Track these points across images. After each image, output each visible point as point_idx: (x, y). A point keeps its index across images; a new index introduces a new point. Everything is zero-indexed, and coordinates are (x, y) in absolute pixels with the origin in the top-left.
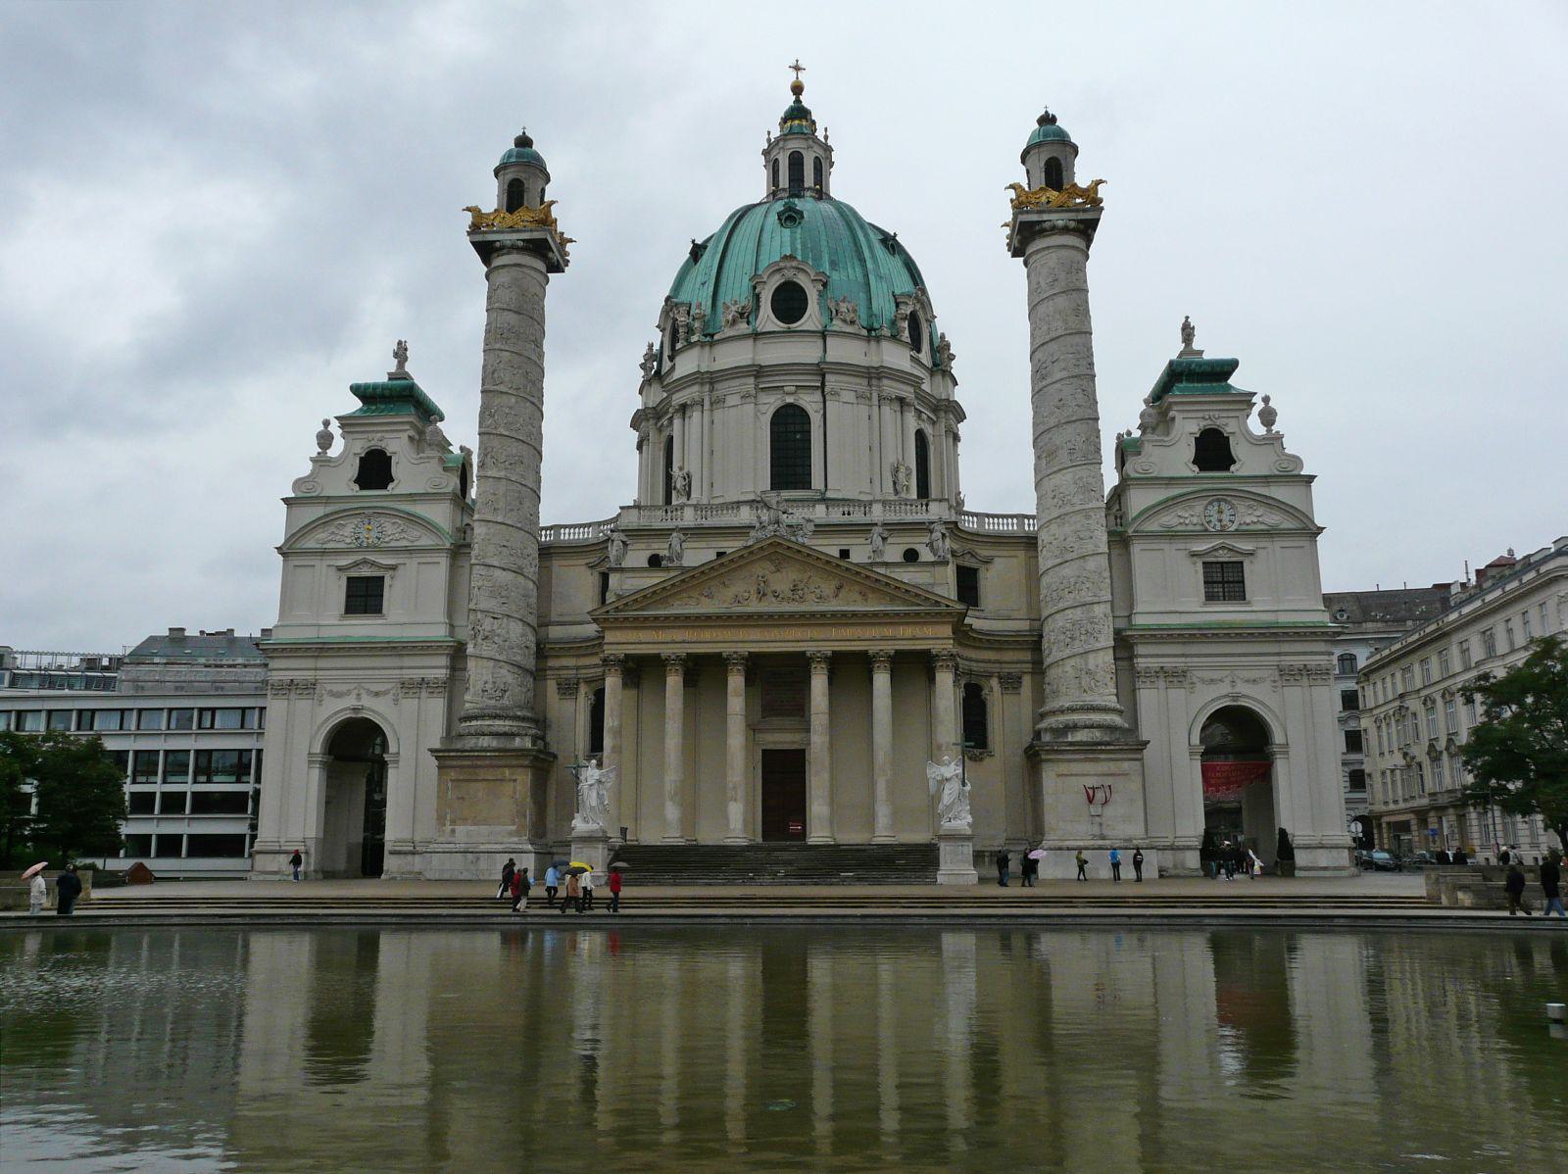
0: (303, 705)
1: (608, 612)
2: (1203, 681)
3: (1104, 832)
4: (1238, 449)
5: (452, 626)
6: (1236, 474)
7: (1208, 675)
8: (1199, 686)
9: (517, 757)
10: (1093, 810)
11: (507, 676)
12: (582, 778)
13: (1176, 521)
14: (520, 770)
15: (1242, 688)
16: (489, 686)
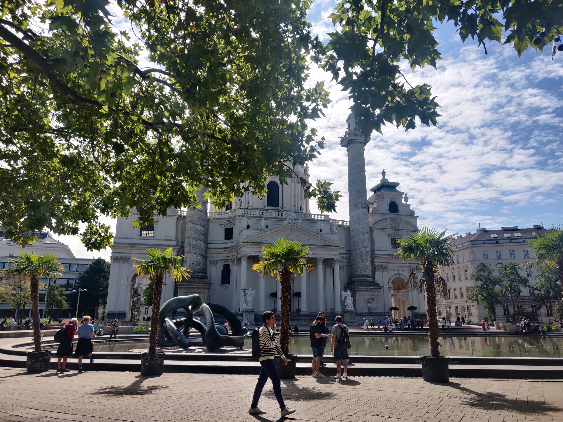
0: (125, 265)
1: (244, 242)
2: (391, 270)
3: (372, 311)
4: (400, 208)
5: (177, 242)
6: (400, 214)
7: (392, 269)
8: (390, 271)
9: (205, 286)
10: (369, 305)
11: (200, 258)
12: (246, 293)
13: (384, 225)
14: (206, 289)
15: (401, 272)
16: (195, 262)
